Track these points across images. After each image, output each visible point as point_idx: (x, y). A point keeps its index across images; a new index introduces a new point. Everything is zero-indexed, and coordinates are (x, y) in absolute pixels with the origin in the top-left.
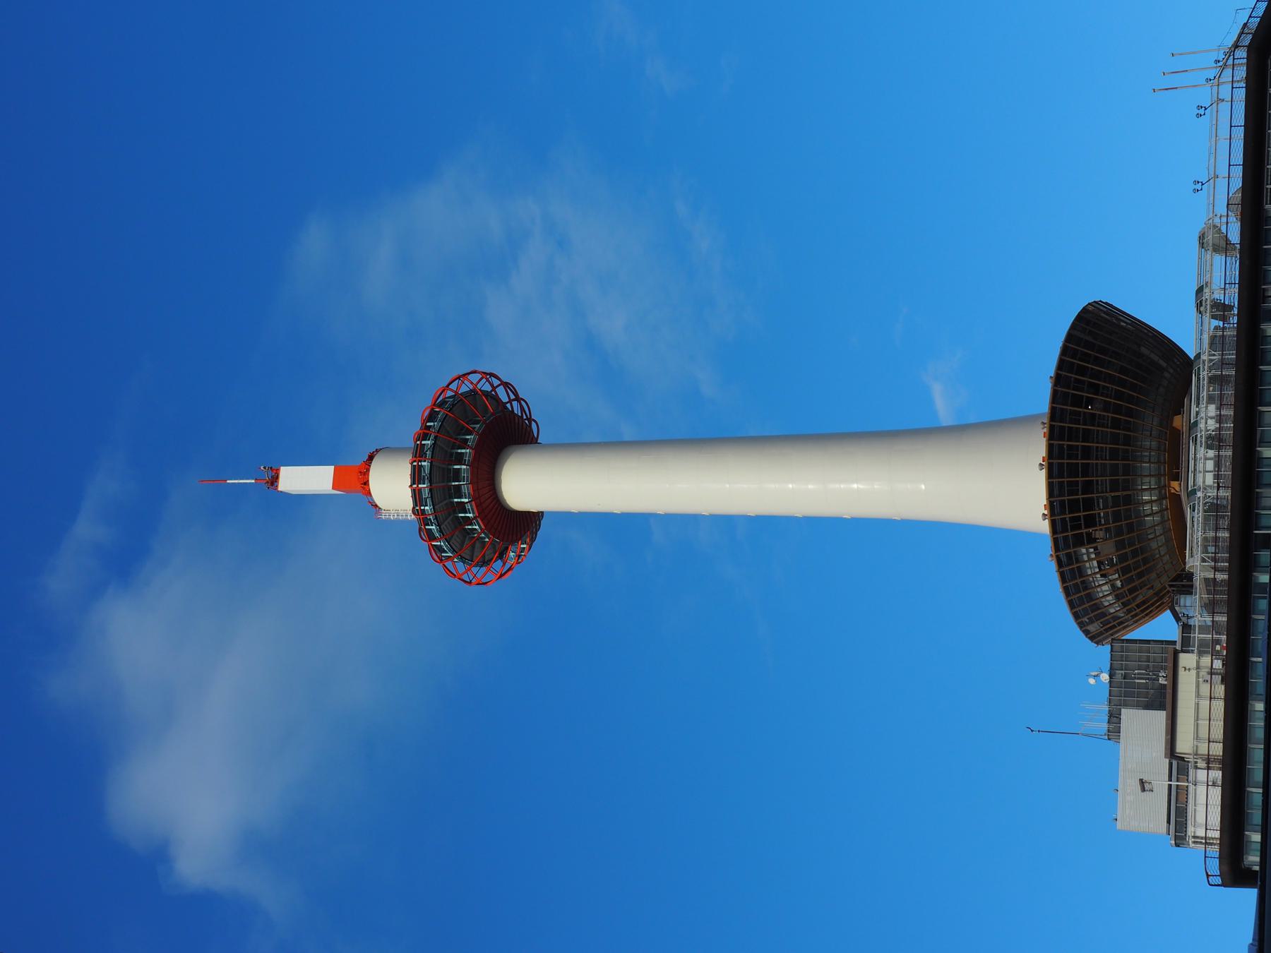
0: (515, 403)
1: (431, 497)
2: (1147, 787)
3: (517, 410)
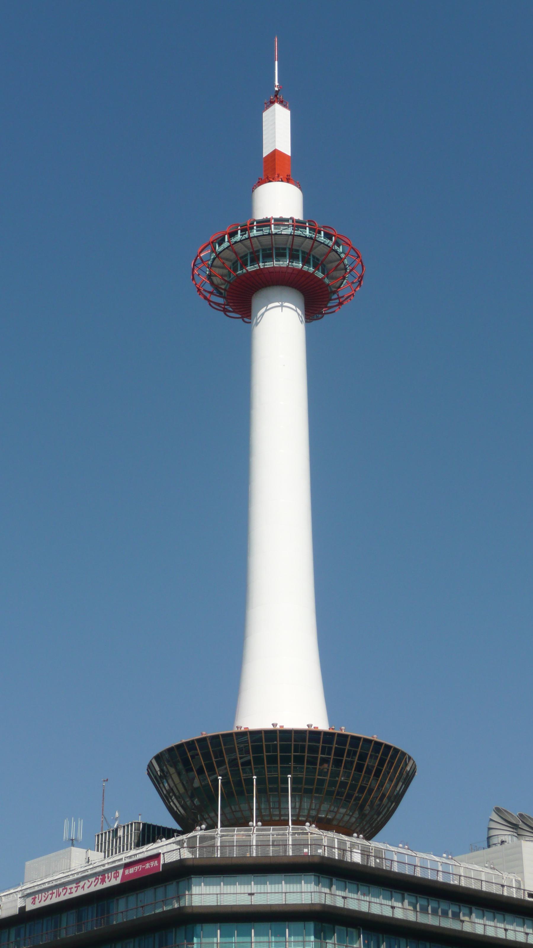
0: (337, 301)
1: (264, 235)
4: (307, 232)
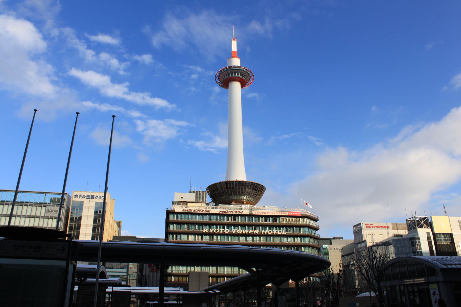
2: (182, 198)
3: (246, 85)
4: (241, 69)
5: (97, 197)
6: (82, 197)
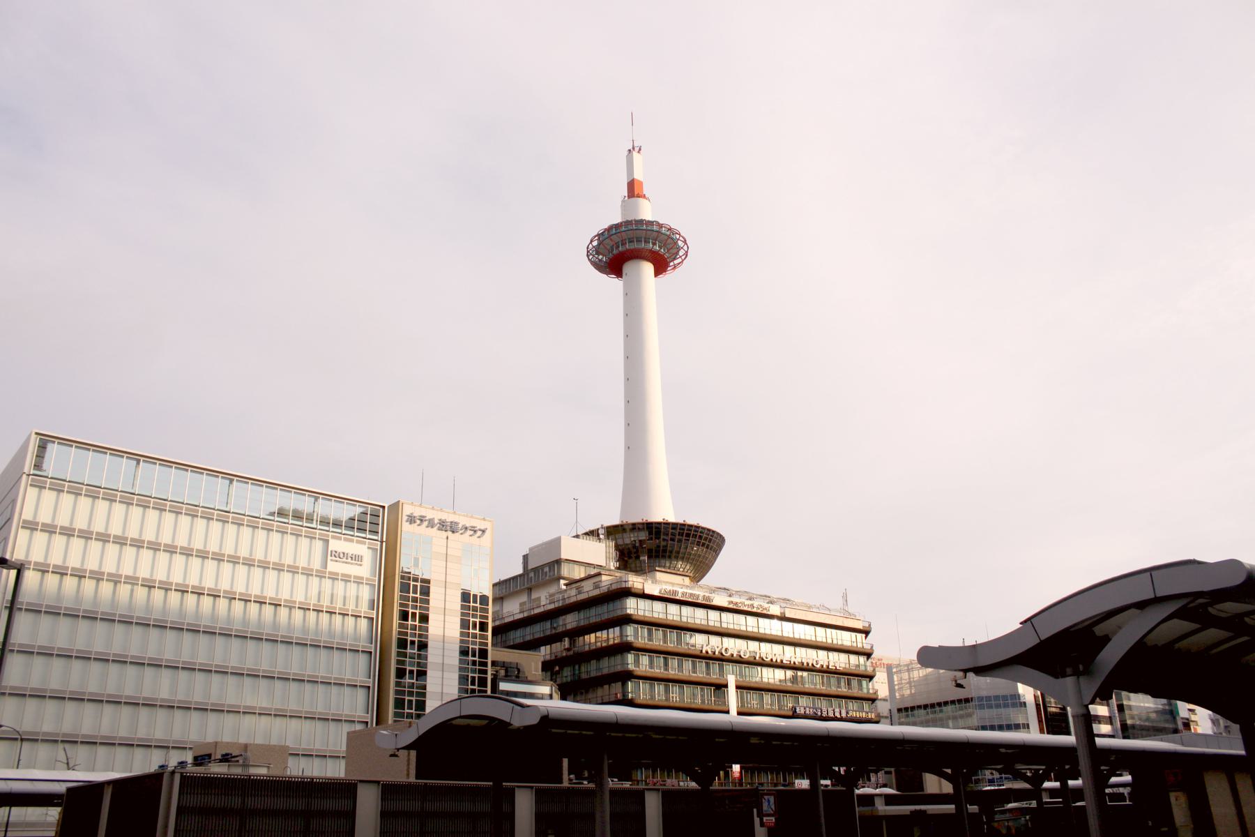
5: (466, 528)
6: (426, 523)
